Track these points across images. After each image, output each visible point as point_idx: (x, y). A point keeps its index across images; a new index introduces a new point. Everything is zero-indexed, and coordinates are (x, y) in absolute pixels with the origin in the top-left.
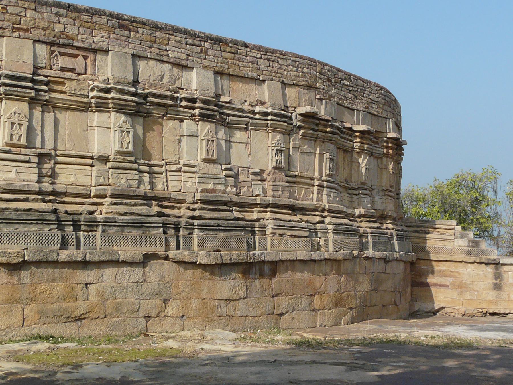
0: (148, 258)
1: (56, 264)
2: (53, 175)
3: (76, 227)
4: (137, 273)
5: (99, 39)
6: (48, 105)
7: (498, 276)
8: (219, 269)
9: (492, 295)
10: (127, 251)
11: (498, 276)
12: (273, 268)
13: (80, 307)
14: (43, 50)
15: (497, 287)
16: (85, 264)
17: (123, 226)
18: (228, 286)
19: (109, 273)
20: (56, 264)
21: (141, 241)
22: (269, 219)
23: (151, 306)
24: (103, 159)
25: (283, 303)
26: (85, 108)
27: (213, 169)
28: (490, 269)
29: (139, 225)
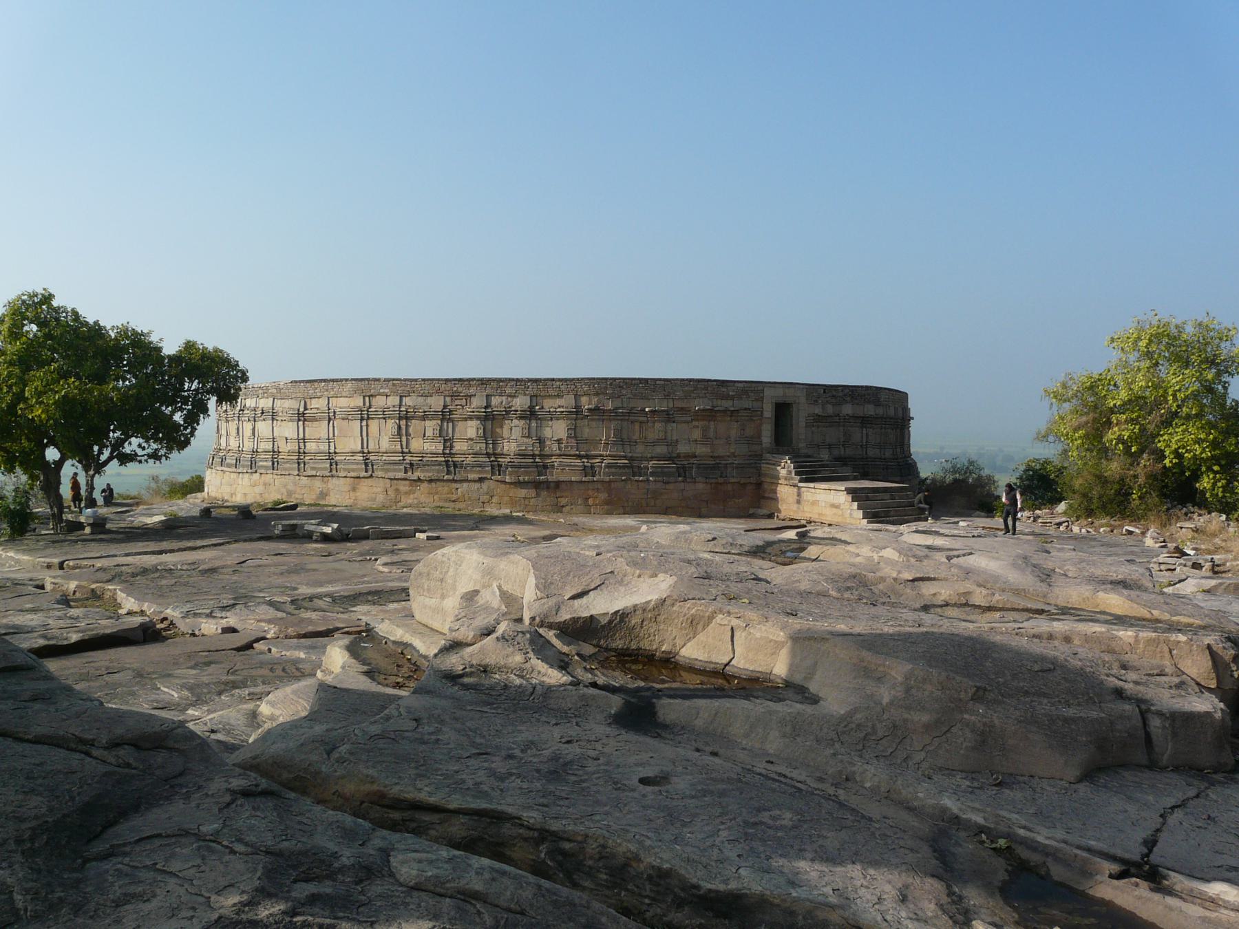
0: (481, 480)
1: (443, 480)
2: (451, 447)
3: (455, 466)
4: (477, 485)
5: (472, 391)
6: (450, 420)
7: (799, 495)
8: (518, 484)
9: (795, 507)
10: (471, 476)
11: (799, 495)
12: (558, 484)
13: (454, 497)
14: (448, 399)
15: (798, 502)
16: (456, 481)
17: (473, 466)
18: (523, 493)
19: (465, 485)
20: (443, 480)
21: (480, 472)
22: (556, 461)
23: (486, 498)
24: (471, 439)
25: (563, 501)
26: (466, 420)
27: (526, 440)
28: (795, 490)
29: (480, 466)
